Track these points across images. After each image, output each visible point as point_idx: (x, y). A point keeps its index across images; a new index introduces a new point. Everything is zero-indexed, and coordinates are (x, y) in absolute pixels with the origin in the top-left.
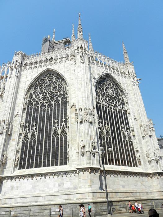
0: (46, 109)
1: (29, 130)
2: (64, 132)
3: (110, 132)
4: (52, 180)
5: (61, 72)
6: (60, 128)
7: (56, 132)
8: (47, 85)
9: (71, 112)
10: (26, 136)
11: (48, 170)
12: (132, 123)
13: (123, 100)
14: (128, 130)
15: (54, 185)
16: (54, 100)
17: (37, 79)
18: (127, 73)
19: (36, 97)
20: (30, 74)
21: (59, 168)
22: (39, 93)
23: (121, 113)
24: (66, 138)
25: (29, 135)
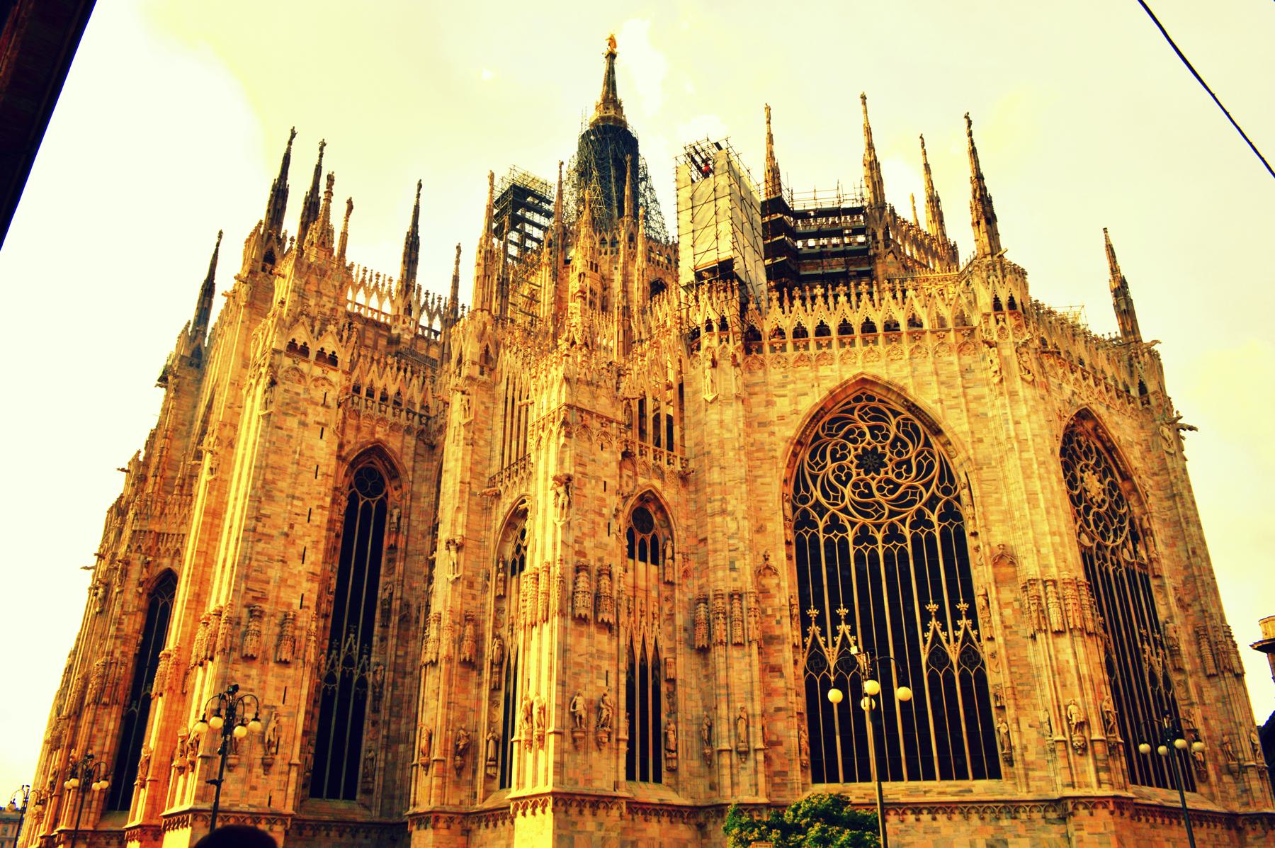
0: (881, 552)
1: (823, 633)
2: (970, 658)
3: (1114, 656)
4: (963, 829)
5: (928, 399)
7: (938, 655)
8: (864, 448)
9: (996, 582)
10: (816, 659)
11: (940, 793)
12: (1171, 617)
13: (1132, 523)
14: (1160, 650)
17: (815, 418)
18: (1134, 392)
20: (783, 386)
21: (981, 788)
22: (838, 478)
23: (1134, 572)
24: (982, 679)
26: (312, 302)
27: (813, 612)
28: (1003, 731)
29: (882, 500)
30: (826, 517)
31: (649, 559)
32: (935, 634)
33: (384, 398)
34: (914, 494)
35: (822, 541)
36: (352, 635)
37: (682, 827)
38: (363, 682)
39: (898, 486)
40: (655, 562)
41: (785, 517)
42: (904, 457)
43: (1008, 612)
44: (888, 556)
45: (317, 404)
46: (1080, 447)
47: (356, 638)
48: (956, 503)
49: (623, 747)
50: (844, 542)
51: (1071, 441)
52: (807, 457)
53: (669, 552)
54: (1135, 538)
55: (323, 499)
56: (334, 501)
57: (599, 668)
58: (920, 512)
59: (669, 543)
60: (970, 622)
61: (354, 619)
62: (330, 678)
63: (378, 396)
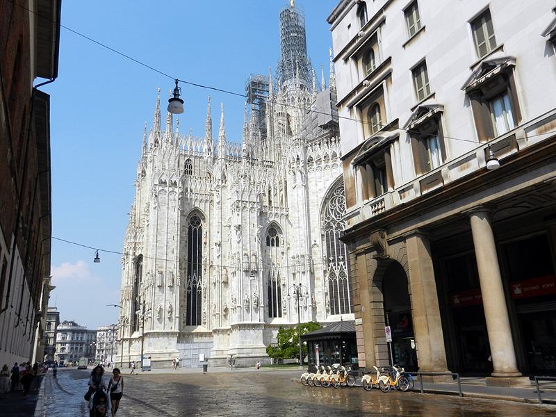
1: (335, 265)
10: (332, 274)
19: (336, 216)
25: (337, 273)
26: (167, 164)
27: (331, 258)
38: (200, 288)
61: (195, 268)
62: (189, 288)
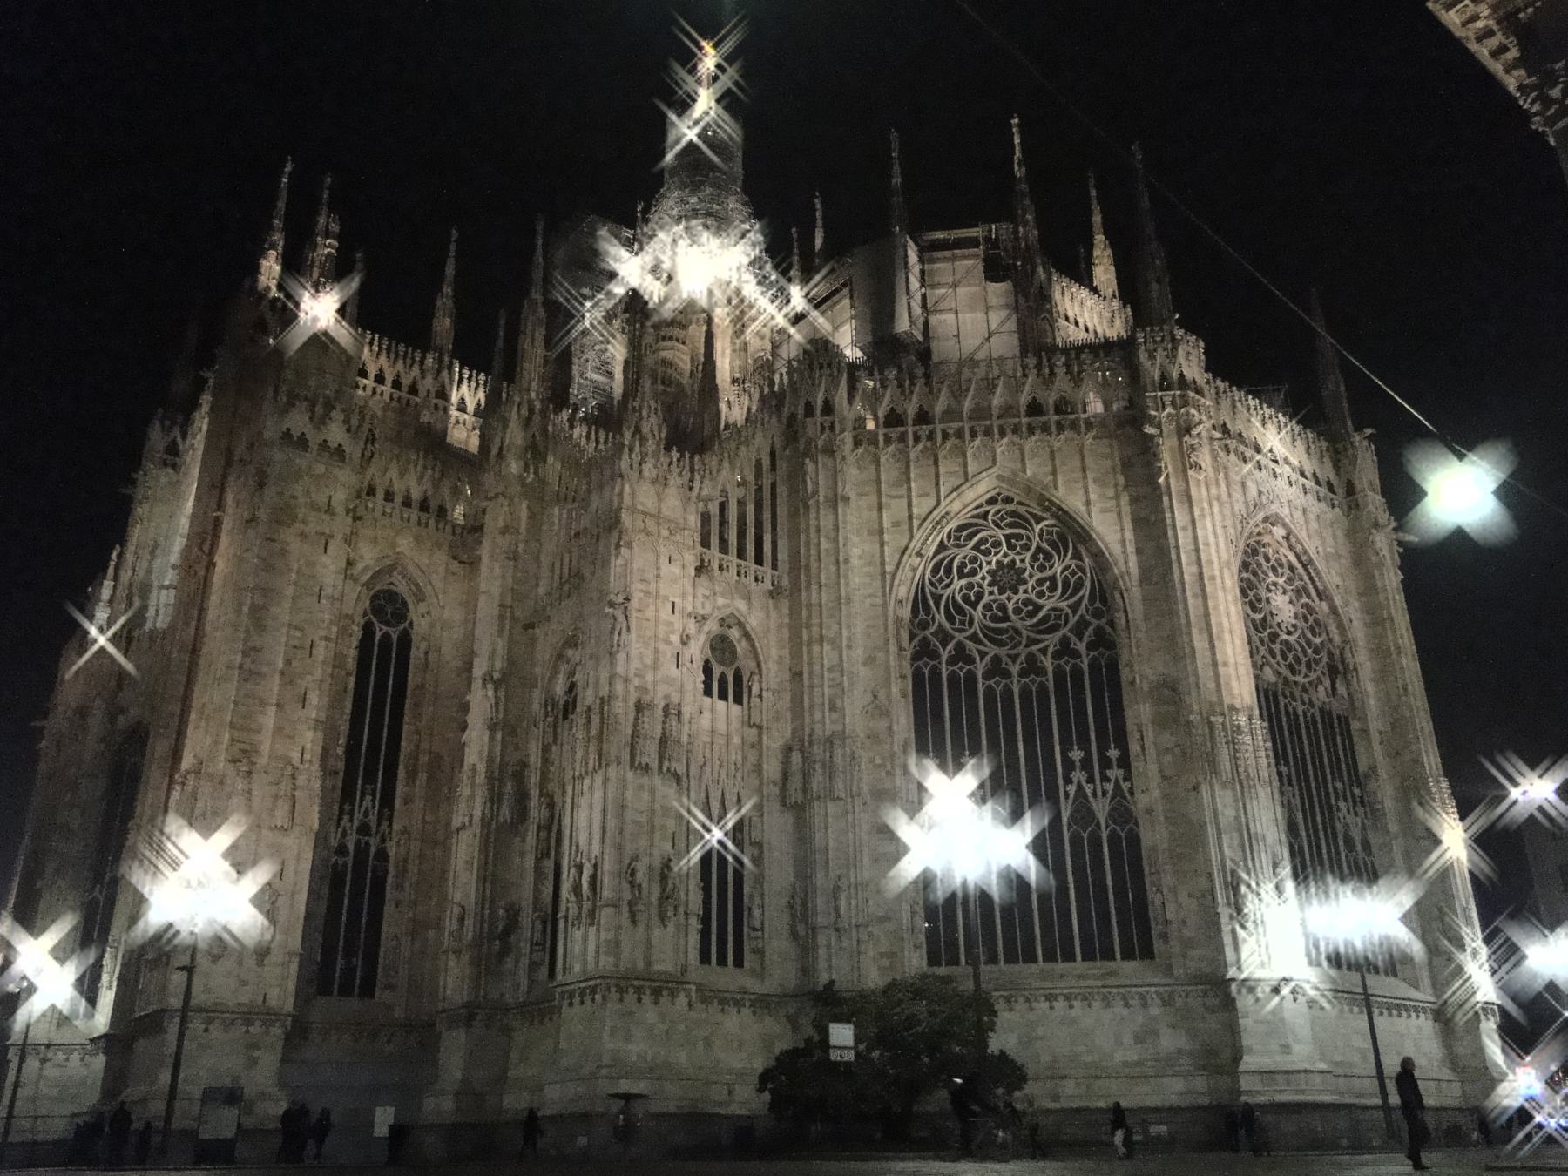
0: (1016, 689)
3: (1300, 815)
6: (1100, 793)
7: (1083, 814)
15: (1119, 1042)
16: (1051, 649)
24: (1134, 841)
28: (1158, 902)
29: (1019, 624)
30: (950, 646)
31: (731, 698)
32: (1080, 786)
33: (407, 503)
34: (1058, 618)
35: (944, 676)
36: (369, 798)
37: (768, 1019)
38: (382, 855)
39: (1038, 608)
40: (738, 700)
41: (901, 649)
42: (1048, 573)
43: (1168, 758)
44: (1025, 694)
45: (318, 510)
46: (1268, 560)
47: (373, 801)
48: (1108, 629)
49: (695, 924)
50: (971, 678)
51: (1255, 552)
52: (928, 572)
53: (755, 690)
54: (1333, 671)
55: (328, 628)
56: (344, 631)
57: (664, 828)
58: (1065, 641)
59: (756, 677)
60: (1121, 772)
61: (370, 777)
62: (341, 850)
63: (398, 499)
